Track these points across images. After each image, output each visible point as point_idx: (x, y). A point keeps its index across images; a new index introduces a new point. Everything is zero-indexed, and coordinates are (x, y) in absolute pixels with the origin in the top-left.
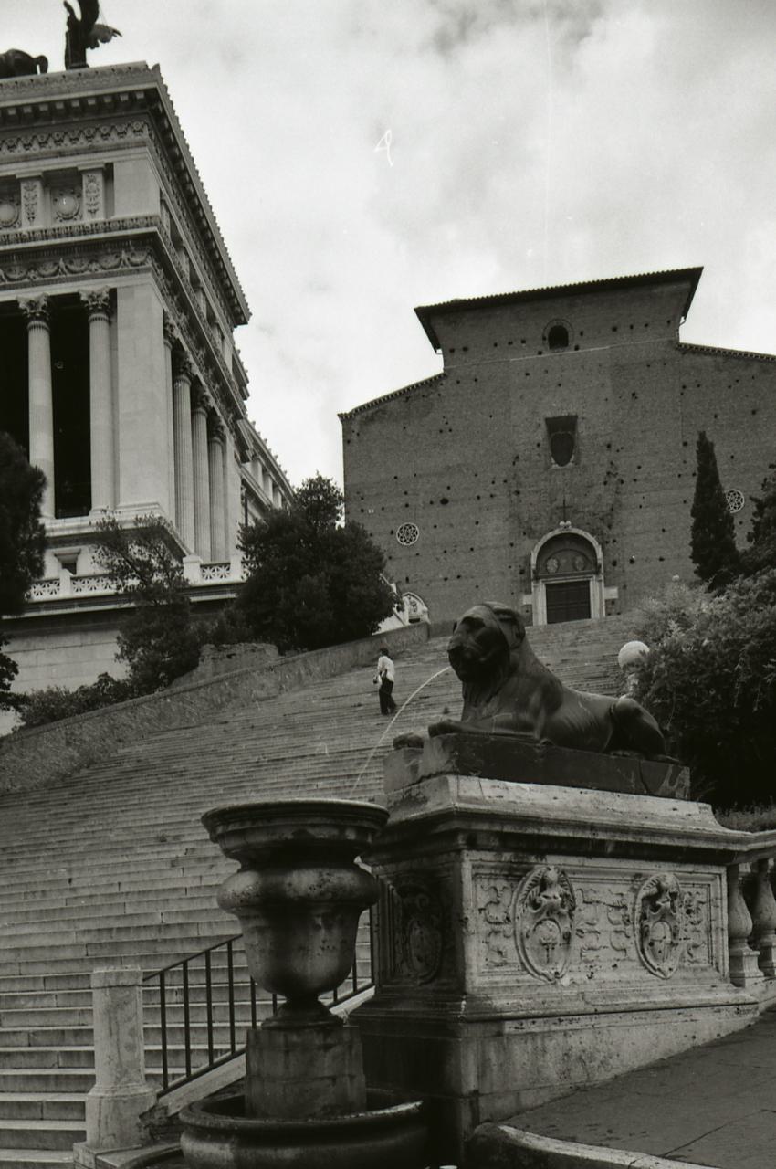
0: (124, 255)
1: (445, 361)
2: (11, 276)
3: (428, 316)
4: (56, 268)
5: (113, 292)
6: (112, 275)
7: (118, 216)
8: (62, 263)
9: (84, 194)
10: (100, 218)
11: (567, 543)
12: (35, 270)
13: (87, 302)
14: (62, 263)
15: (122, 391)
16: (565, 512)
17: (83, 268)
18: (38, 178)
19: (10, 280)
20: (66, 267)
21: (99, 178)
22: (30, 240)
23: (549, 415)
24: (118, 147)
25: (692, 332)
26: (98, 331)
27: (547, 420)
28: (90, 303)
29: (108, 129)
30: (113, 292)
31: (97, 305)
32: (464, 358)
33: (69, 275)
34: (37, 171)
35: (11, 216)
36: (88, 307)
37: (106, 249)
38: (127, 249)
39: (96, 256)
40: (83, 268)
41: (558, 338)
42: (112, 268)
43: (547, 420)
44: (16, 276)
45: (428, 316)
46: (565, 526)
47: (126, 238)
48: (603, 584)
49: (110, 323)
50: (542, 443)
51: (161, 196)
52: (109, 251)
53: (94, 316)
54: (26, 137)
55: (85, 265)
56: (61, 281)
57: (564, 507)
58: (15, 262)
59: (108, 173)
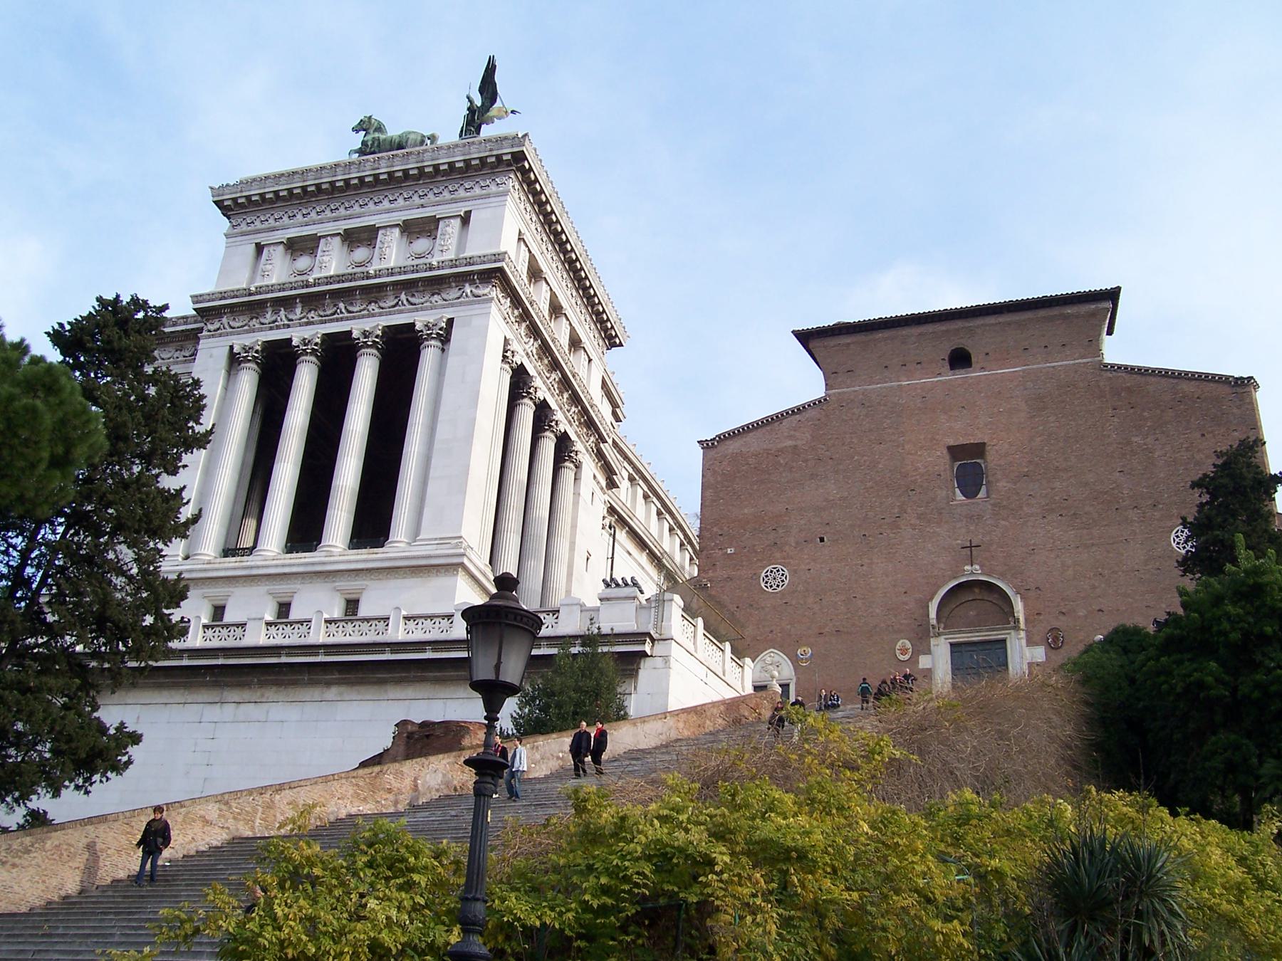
0: (468, 289)
1: (826, 385)
2: (351, 308)
3: (805, 337)
4: (397, 300)
5: (450, 322)
6: (453, 305)
7: (467, 254)
8: (403, 297)
9: (438, 236)
10: (450, 255)
11: (977, 590)
12: (376, 302)
13: (422, 331)
14: (342, 305)
15: (442, 417)
16: (971, 551)
17: (424, 299)
18: (398, 225)
19: (349, 312)
20: (407, 300)
21: (456, 223)
22: (376, 277)
23: (952, 442)
24: (481, 197)
25: (1115, 350)
26: (429, 356)
27: (951, 449)
28: (425, 332)
29: (472, 184)
30: (450, 322)
31: (431, 334)
32: (849, 381)
33: (409, 307)
34: (398, 220)
35: (366, 257)
36: (422, 335)
37: (450, 283)
38: (472, 282)
39: (439, 290)
40: (424, 299)
41: (960, 359)
42: (453, 299)
43: (951, 449)
44: (355, 309)
45: (805, 337)
46: (973, 572)
47: (472, 273)
48: (1024, 642)
49: (443, 350)
50: (942, 473)
51: (519, 235)
52: (453, 284)
53: (426, 343)
54: (393, 194)
55: (427, 298)
56: (401, 312)
57: (971, 547)
58: (358, 297)
59: (466, 219)
